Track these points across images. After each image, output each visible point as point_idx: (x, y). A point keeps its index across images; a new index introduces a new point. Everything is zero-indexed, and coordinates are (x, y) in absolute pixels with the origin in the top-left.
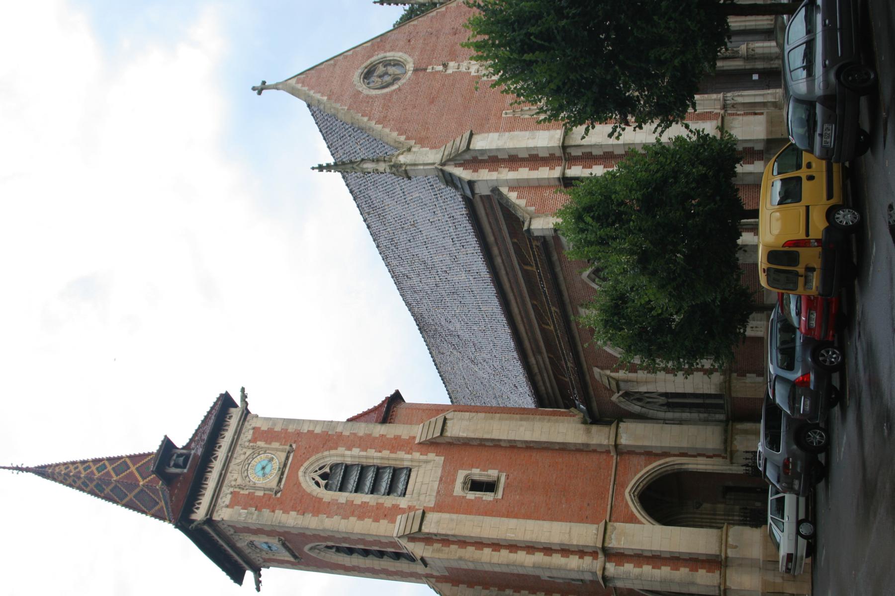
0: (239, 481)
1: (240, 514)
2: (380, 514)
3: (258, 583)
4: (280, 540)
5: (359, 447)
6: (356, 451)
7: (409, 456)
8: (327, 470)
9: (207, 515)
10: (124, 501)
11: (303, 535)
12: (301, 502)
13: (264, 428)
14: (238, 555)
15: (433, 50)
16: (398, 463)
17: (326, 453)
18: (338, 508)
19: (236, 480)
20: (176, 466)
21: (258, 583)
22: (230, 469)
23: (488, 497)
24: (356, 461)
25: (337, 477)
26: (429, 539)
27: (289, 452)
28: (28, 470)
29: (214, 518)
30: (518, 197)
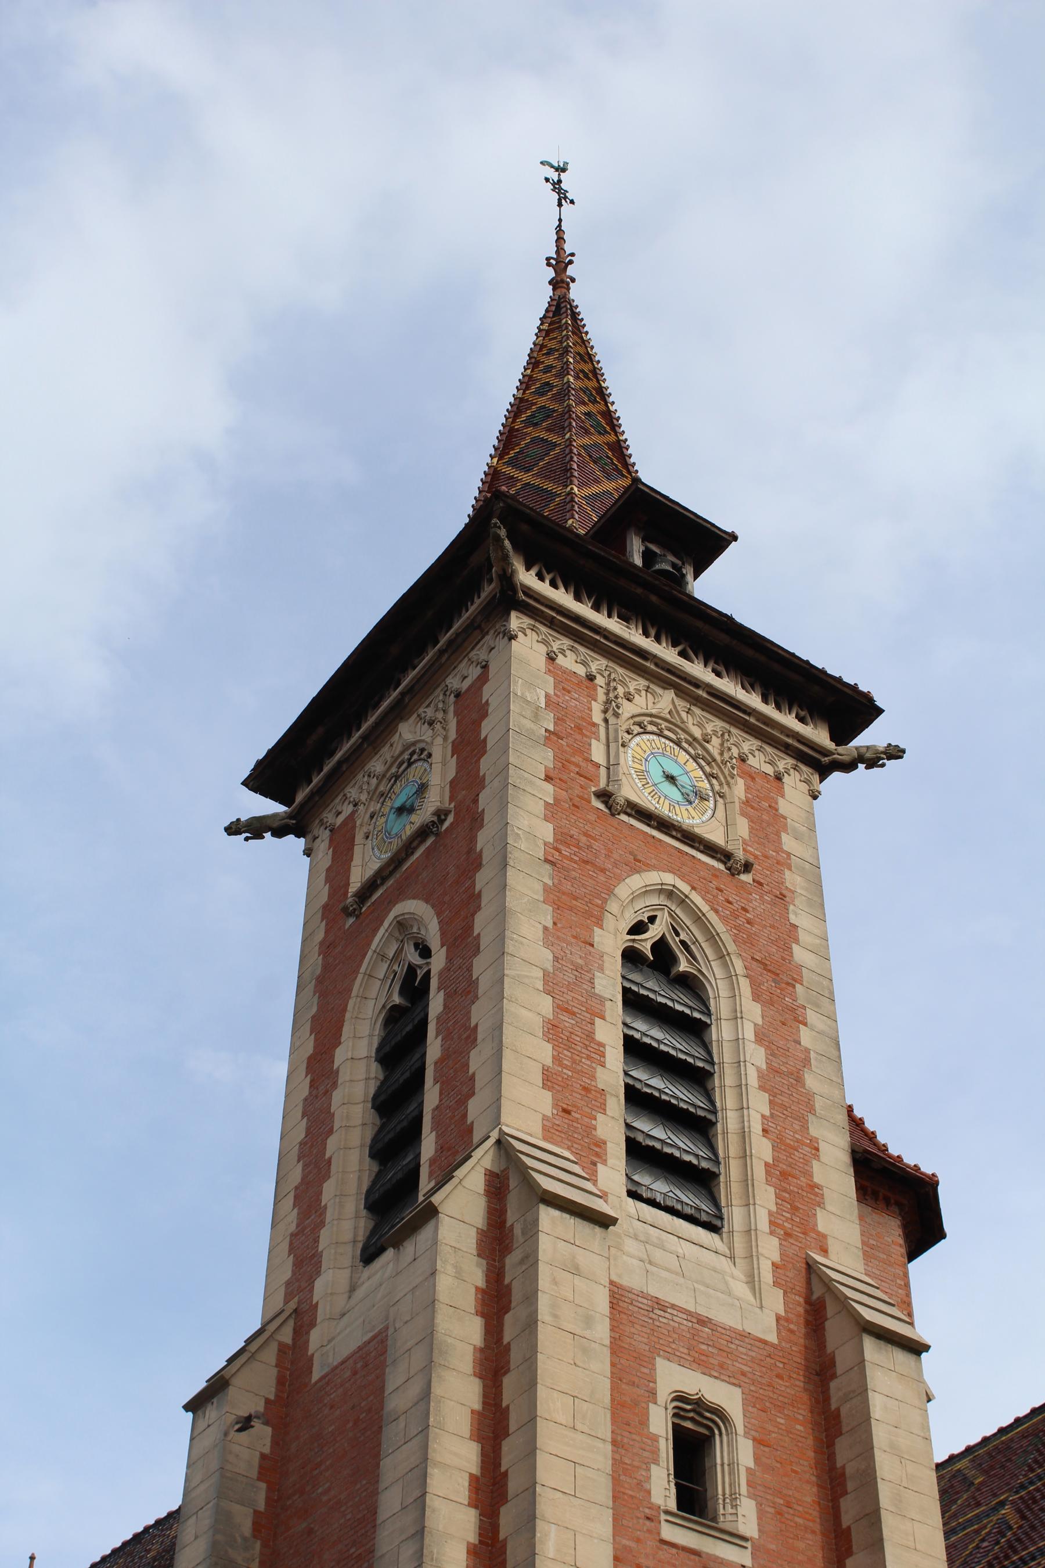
0: (628, 709)
1: (530, 685)
2: (571, 1086)
3: (254, 829)
4: (441, 815)
6: (756, 1056)
7: (763, 1223)
9: (528, 591)
10: (508, 470)
11: (475, 863)
12: (587, 862)
13: (784, 807)
14: (365, 738)
16: (736, 1188)
17: (739, 965)
18: (577, 968)
21: (254, 829)
22: (659, 691)
23: (662, 1486)
24: (723, 1054)
25: (664, 987)
26: (502, 1242)
29: (514, 614)
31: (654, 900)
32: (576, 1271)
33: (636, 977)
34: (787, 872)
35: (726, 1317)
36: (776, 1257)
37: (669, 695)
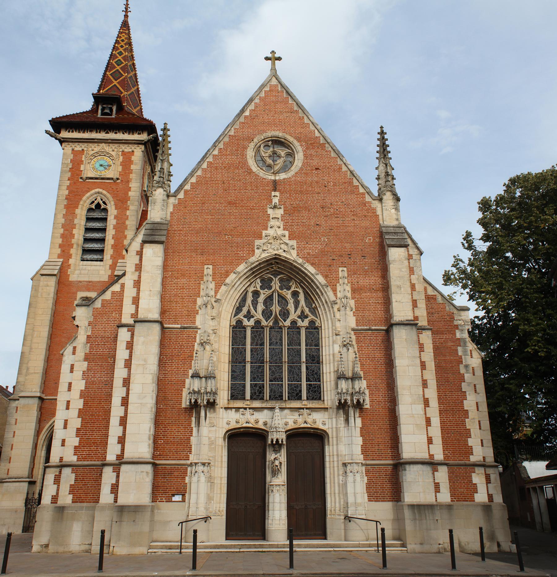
5: (117, 223)
8: (103, 206)
9: (63, 138)
15: (301, 192)
17: (113, 203)
20: (103, 109)
27: (112, 179)
28: (126, 16)
30: (113, 293)
31: (95, 195)
32: (48, 286)
34: (131, 175)
35: (95, 279)
36: (111, 263)
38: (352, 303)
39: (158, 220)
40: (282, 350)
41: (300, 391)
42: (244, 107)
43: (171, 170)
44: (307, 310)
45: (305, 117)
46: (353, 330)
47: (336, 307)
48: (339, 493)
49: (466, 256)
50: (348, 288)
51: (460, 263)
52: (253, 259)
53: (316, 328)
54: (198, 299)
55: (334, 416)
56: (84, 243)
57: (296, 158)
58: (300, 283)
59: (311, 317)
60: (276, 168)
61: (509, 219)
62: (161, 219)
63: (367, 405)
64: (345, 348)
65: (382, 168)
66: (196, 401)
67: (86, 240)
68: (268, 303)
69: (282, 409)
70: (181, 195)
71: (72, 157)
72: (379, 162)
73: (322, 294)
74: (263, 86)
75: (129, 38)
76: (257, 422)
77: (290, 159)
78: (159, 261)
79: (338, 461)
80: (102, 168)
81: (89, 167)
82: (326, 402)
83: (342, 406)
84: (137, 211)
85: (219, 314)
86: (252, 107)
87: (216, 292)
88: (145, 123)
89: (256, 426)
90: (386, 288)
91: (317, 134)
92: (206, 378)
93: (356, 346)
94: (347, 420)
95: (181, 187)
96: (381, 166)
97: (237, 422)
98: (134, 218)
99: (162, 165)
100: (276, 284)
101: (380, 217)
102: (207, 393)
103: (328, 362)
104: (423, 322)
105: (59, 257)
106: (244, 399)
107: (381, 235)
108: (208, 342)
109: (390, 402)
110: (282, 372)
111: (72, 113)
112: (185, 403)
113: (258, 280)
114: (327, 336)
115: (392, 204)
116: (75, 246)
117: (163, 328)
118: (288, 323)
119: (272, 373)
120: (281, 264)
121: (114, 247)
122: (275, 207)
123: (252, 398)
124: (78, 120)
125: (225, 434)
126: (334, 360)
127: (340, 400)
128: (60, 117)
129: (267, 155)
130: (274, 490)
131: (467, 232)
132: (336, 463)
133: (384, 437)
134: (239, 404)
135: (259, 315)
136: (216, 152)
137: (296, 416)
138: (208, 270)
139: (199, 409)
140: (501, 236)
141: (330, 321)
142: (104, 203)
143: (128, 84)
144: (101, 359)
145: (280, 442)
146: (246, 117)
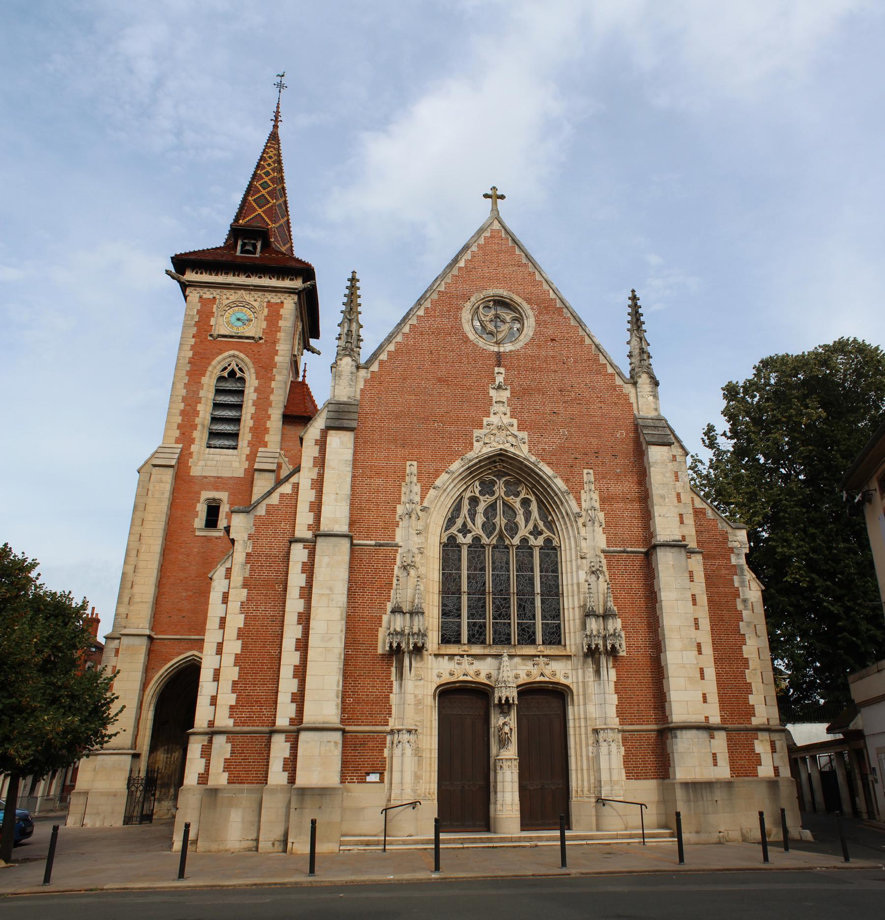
5: (258, 398)
9: (188, 281)
15: (533, 369)
17: (253, 370)
19: (228, 299)
27: (253, 338)
33: (222, 384)
35: (227, 474)
36: (248, 453)
37: (242, 291)
38: (601, 516)
39: (345, 399)
40: (509, 577)
41: (534, 633)
42: (457, 256)
43: (361, 333)
44: (541, 525)
45: (537, 273)
46: (603, 551)
47: (580, 521)
48: (588, 770)
49: (707, 455)
50: (596, 496)
51: (699, 464)
52: (471, 455)
53: (554, 548)
54: (398, 506)
55: (580, 667)
56: (211, 423)
57: (526, 325)
58: (532, 488)
59: (547, 533)
60: (500, 336)
61: (759, 408)
62: (349, 398)
63: (623, 653)
64: (593, 576)
65: (636, 343)
66: (399, 645)
67: (215, 420)
68: (490, 514)
69: (511, 656)
70: (375, 367)
71: (199, 306)
72: (631, 334)
73: (562, 503)
74: (481, 230)
75: (279, 155)
76: (478, 674)
77: (517, 326)
78: (348, 455)
79: (586, 727)
80: (240, 323)
81: (220, 320)
82: (568, 647)
83: (592, 653)
84: (286, 383)
85: (427, 527)
86: (468, 256)
87: (423, 498)
88: (294, 264)
89: (477, 680)
90: (644, 498)
91: (552, 295)
92: (411, 614)
93: (607, 573)
94: (598, 672)
95: (375, 355)
96: (633, 340)
97: (451, 674)
98: (281, 392)
99: (350, 327)
100: (500, 489)
101: (635, 405)
102: (413, 635)
103: (570, 594)
104: (693, 544)
105: (176, 442)
106: (458, 641)
107: (636, 426)
108: (412, 565)
109: (652, 648)
110: (509, 607)
111: (201, 249)
112: (382, 648)
113: (477, 483)
114: (568, 559)
115: (650, 389)
116: (199, 427)
117: (352, 544)
118: (516, 541)
119: (497, 608)
120: (507, 462)
121: (253, 430)
122: (499, 387)
123: (470, 642)
124: (210, 258)
125: (436, 690)
126: (579, 592)
127: (589, 645)
128: (186, 254)
129: (488, 319)
130: (504, 767)
131: (708, 425)
132: (583, 729)
133: (644, 694)
134: (453, 649)
135: (478, 530)
136: (421, 312)
137: (529, 666)
138: (412, 468)
139: (401, 656)
140: (754, 432)
141: (572, 539)
142: (241, 370)
143: (276, 213)
144: (267, 585)
145: (511, 702)
146: (460, 268)
